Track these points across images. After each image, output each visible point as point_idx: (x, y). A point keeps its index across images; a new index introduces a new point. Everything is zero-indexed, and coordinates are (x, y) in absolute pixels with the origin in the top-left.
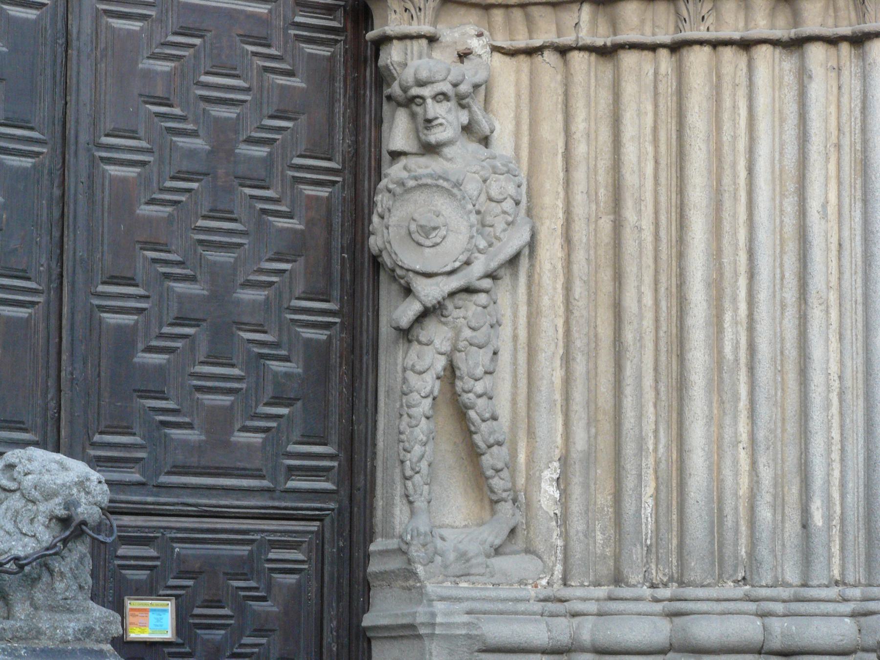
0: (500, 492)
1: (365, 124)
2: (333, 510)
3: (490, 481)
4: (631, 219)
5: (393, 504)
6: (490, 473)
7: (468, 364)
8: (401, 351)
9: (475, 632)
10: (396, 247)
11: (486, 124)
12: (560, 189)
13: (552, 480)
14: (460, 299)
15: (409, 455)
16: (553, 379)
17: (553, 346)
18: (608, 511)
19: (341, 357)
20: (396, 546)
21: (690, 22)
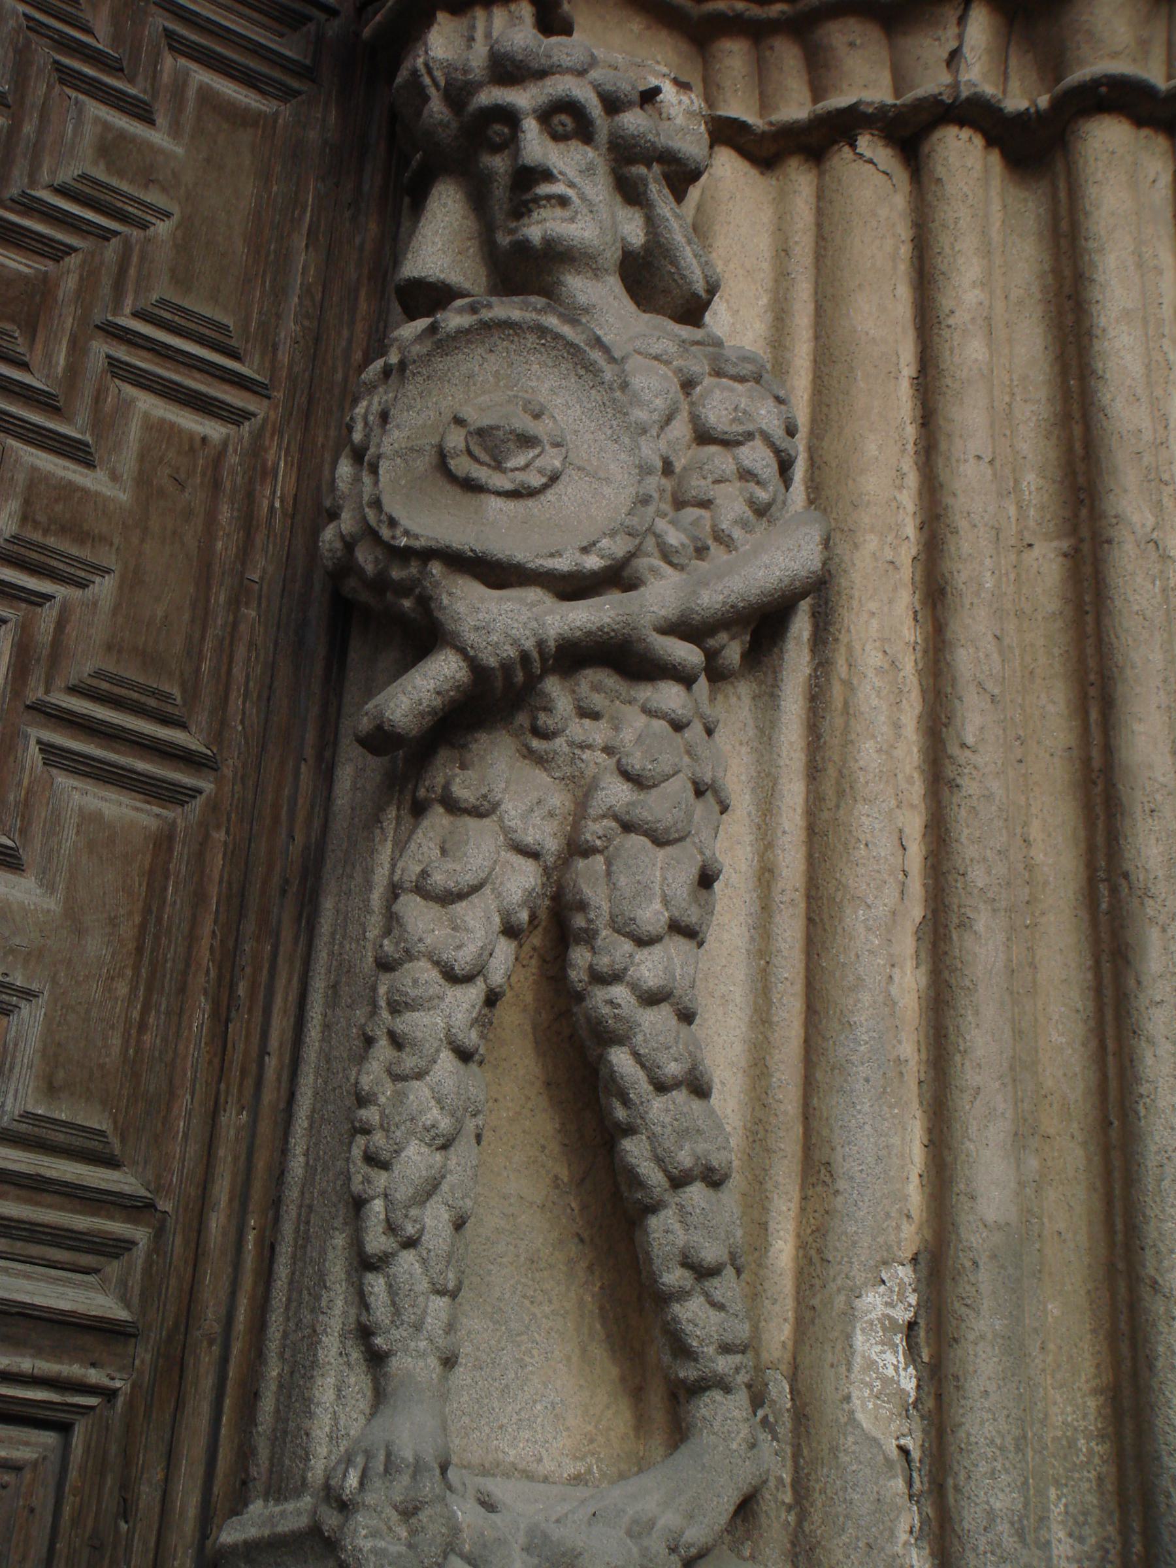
0: (710, 1350)
2: (109, 1394)
3: (676, 1308)
4: (1135, 518)
5: (314, 1364)
6: (674, 1277)
7: (613, 886)
8: (389, 844)
10: (393, 506)
11: (694, 262)
12: (908, 464)
13: (890, 1325)
14: (596, 688)
15: (381, 1179)
16: (894, 990)
17: (890, 894)
18: (1091, 1451)
20: (303, 1522)
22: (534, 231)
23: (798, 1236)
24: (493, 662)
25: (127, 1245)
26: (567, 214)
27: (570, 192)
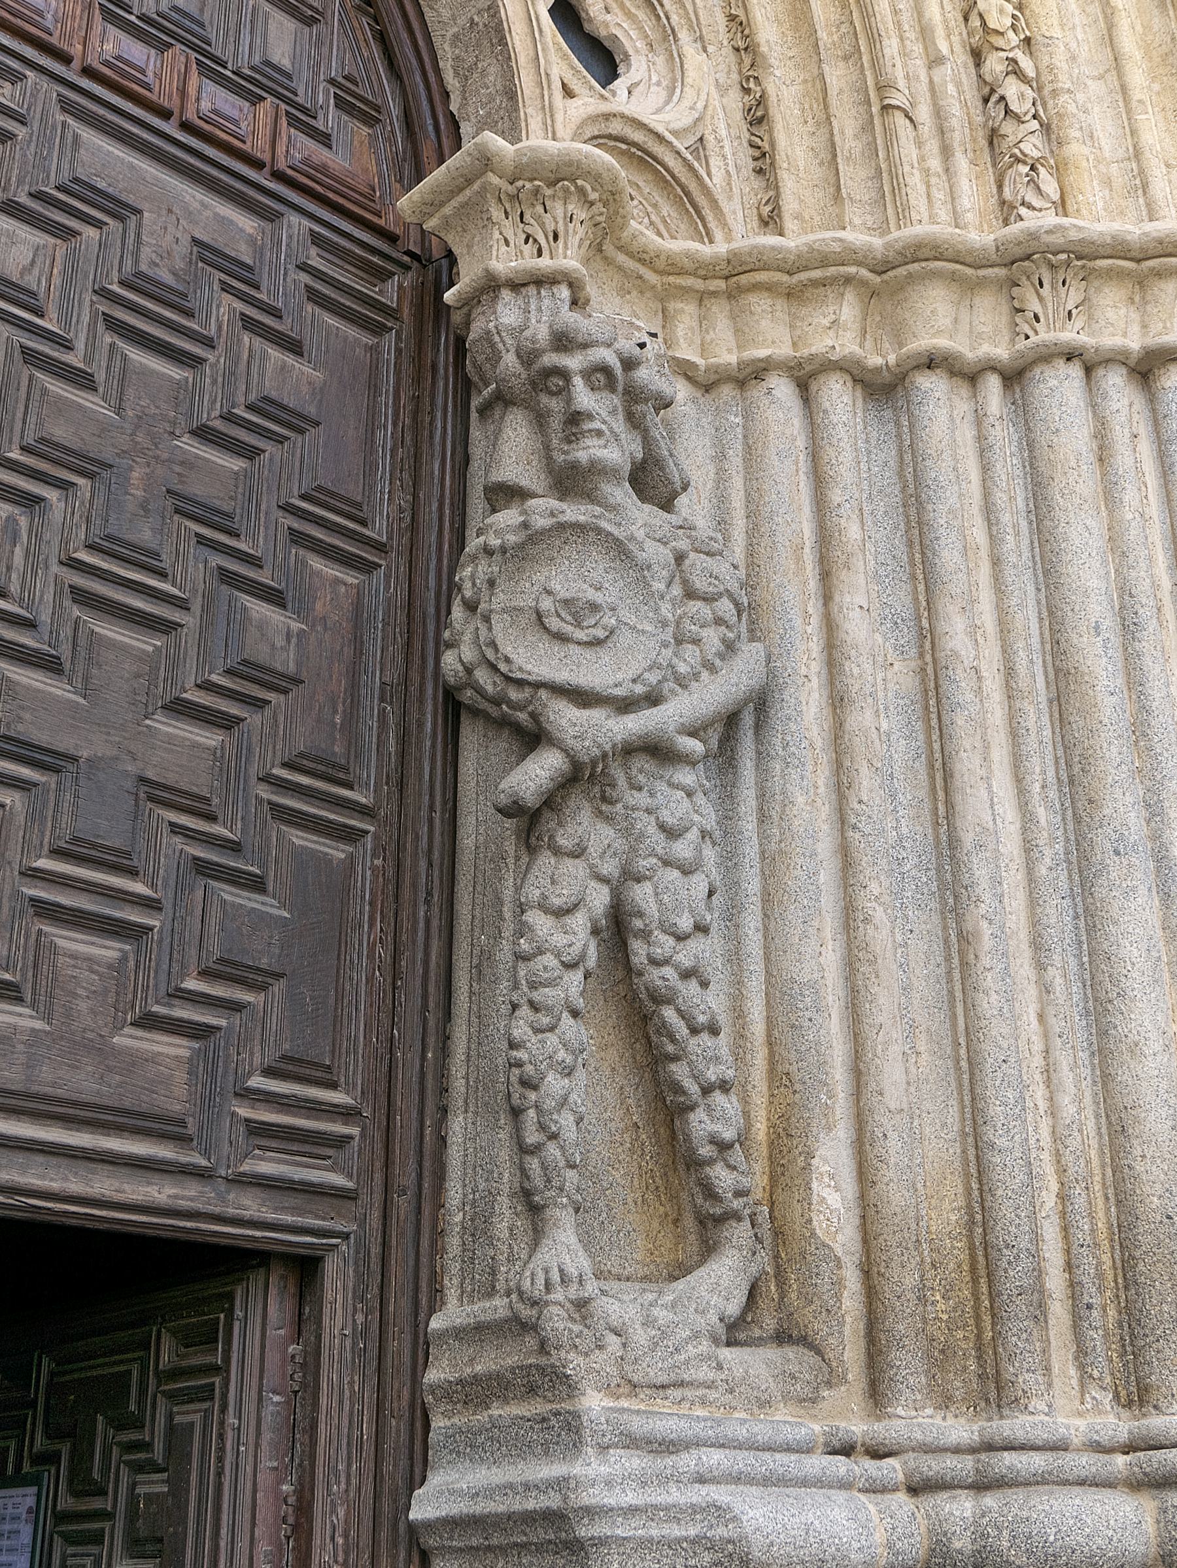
1: (432, 473)
2: (345, 1236)
6: (706, 1151)
9: (721, 1532)
15: (533, 1096)
19: (372, 903)
20: (502, 1313)
21: (1047, 319)
22: (582, 456)
23: (769, 1119)
24: (586, 759)
25: (351, 1137)
26: (602, 442)
27: (604, 427)
